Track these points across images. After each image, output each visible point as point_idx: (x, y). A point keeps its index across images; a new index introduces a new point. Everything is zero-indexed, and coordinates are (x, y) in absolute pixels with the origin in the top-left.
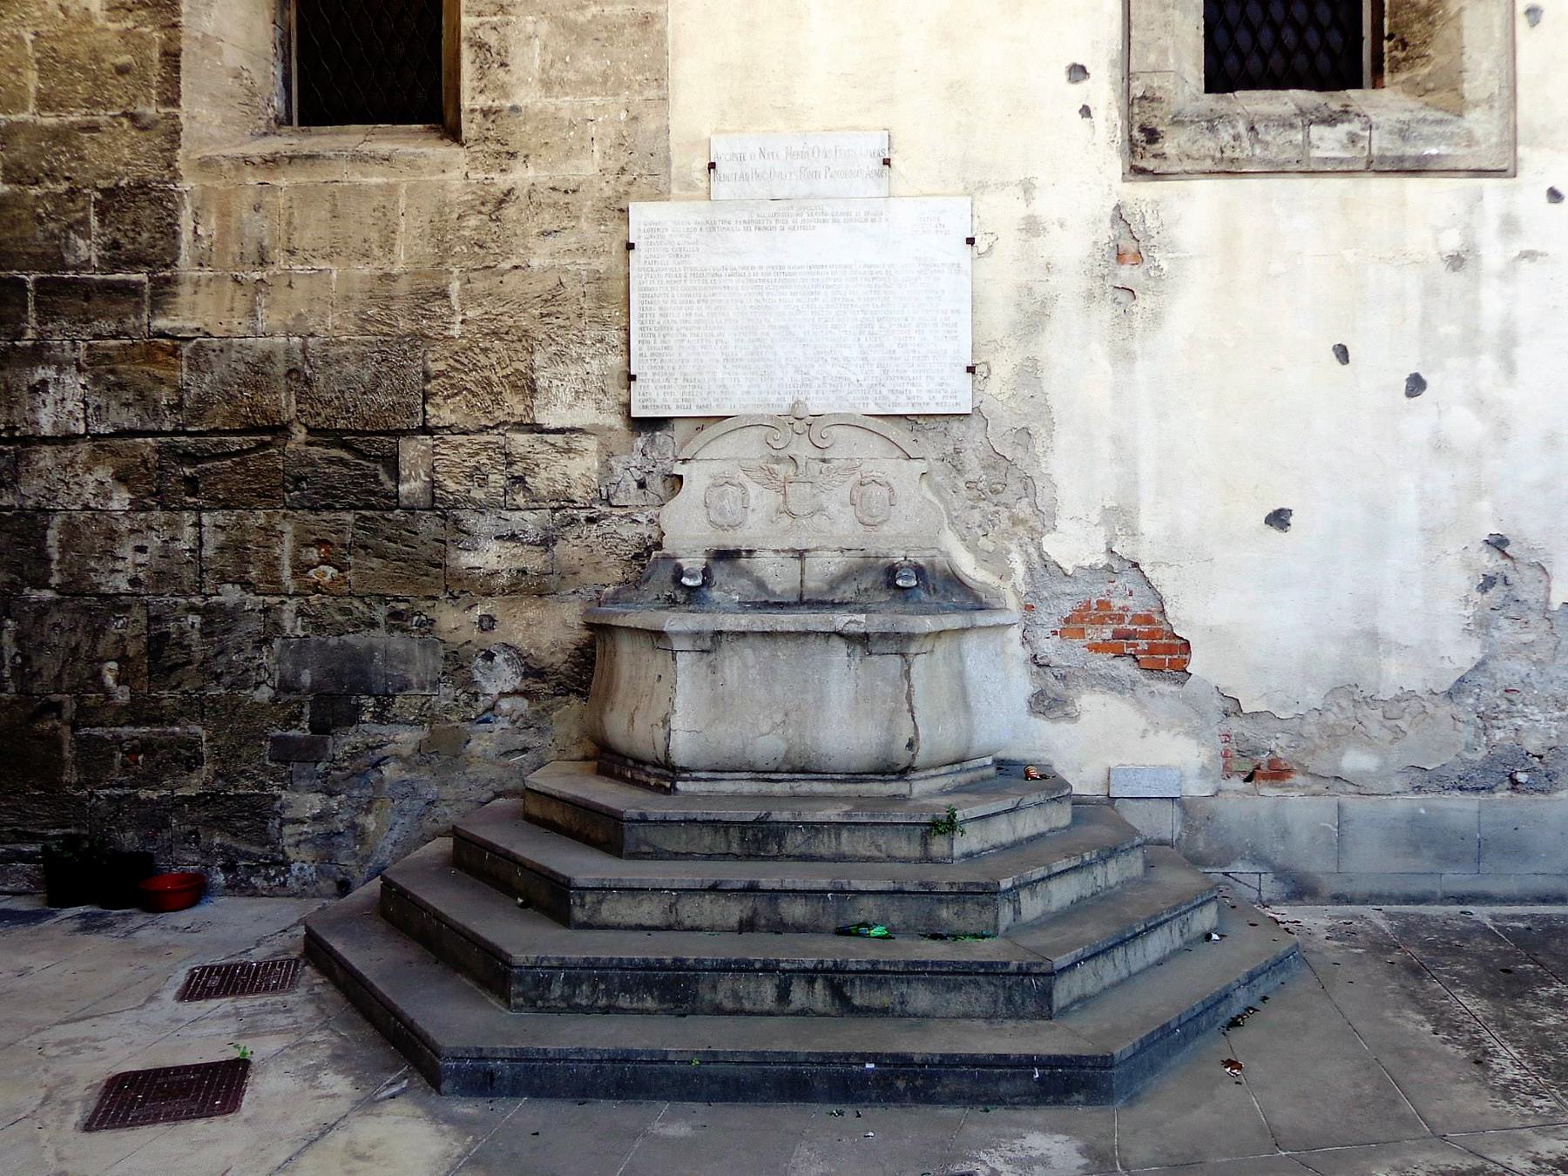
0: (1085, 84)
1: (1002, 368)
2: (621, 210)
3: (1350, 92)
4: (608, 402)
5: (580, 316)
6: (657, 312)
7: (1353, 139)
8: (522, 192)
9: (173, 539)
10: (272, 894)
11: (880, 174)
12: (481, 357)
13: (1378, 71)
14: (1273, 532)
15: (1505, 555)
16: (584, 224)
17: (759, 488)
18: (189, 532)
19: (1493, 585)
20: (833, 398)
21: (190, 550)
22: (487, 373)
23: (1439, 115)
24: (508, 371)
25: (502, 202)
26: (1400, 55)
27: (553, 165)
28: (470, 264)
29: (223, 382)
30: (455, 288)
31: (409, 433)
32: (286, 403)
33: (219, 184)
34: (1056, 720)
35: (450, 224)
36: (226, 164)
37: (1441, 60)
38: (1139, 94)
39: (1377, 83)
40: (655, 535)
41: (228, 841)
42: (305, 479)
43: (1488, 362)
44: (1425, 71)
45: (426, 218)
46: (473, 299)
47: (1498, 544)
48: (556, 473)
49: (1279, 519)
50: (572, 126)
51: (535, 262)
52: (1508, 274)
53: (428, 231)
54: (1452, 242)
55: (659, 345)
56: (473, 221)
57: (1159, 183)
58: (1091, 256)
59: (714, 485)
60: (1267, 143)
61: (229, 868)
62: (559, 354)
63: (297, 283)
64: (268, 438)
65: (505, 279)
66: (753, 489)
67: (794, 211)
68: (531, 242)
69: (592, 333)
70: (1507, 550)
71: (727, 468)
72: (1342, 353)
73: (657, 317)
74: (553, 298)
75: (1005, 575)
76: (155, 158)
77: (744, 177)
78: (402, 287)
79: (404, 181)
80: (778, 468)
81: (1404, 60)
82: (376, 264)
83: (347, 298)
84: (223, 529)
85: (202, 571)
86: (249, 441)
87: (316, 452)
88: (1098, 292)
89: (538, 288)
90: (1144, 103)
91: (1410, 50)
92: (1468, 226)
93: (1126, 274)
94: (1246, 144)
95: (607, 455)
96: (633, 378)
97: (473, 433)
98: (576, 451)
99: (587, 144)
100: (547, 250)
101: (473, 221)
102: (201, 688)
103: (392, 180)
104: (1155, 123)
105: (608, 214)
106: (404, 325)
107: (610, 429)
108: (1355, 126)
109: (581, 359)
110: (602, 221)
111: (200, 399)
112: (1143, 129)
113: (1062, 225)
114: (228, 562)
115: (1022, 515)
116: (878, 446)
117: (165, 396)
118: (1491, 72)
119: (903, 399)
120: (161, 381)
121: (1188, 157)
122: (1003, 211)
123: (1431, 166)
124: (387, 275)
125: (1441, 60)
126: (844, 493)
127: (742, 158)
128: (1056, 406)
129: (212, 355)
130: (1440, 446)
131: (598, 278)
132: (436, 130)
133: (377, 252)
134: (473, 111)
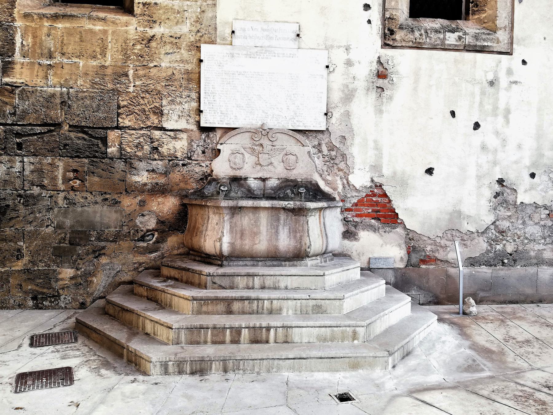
0: (369, 11)
1: (336, 115)
2: (197, 47)
3: (458, 21)
4: (191, 120)
5: (181, 87)
6: (211, 87)
7: (460, 38)
8: (158, 36)
9: (11, 167)
10: (53, 308)
11: (295, 40)
12: (141, 100)
13: (467, 13)
14: (428, 176)
15: (503, 186)
16: (183, 51)
17: (249, 155)
18: (18, 165)
19: (499, 196)
20: (276, 122)
21: (19, 172)
22: (144, 107)
23: (488, 32)
24: (152, 106)
25: (150, 40)
26: (476, 9)
27: (170, 27)
28: (137, 63)
29: (33, 105)
30: (131, 73)
31: (113, 128)
32: (58, 114)
33: (33, 25)
34: (351, 241)
35: (129, 48)
36: (35, 17)
37: (490, 12)
38: (388, 17)
39: (466, 19)
40: (209, 171)
41: (34, 287)
42: (68, 145)
43: (500, 119)
44: (484, 15)
45: (120, 44)
46: (138, 77)
47: (501, 182)
48: (171, 146)
49: (430, 171)
50: (179, 12)
51: (163, 65)
52: (508, 89)
53: (120, 49)
54: (490, 77)
55: (212, 99)
56: (139, 47)
57: (393, 50)
58: (369, 75)
59: (233, 154)
60: (431, 37)
61: (34, 298)
62: (172, 101)
63: (66, 67)
64: (53, 128)
65: (151, 70)
66: (247, 156)
67: (263, 52)
68: (162, 56)
69: (185, 93)
70: (504, 184)
71: (238, 147)
72: (453, 114)
73: (211, 89)
74: (170, 79)
75: (335, 189)
76: (4, 11)
77: (245, 38)
78: (109, 71)
79: (110, 29)
80: (256, 149)
81: (477, 11)
82: (99, 61)
83: (86, 74)
84: (33, 164)
85: (24, 180)
86: (45, 129)
87: (72, 135)
88: (371, 88)
89: (164, 75)
90: (390, 20)
91: (479, 8)
92: (496, 71)
93: (380, 83)
94: (424, 37)
95: (191, 141)
96: (202, 112)
97: (137, 130)
98: (178, 138)
99: (184, 20)
100: (168, 60)
101: (139, 47)
102: (23, 227)
103: (106, 28)
104: (393, 28)
105: (192, 48)
106: (110, 86)
107: (192, 131)
108: (461, 34)
109: (181, 103)
110: (190, 50)
111: (23, 111)
112: (389, 30)
113: (359, 63)
114: (35, 177)
115: (342, 168)
116: (293, 141)
117: (8, 109)
118: (506, 18)
119: (301, 124)
120: (7, 103)
121: (404, 41)
122: (338, 57)
123: (485, 49)
124: (103, 66)
125: (490, 12)
126: (280, 157)
127: (244, 30)
128: (355, 129)
129: (28, 94)
130: (484, 148)
131: (187, 72)
132: (121, 9)
133: (99, 56)
134: (139, 3)
